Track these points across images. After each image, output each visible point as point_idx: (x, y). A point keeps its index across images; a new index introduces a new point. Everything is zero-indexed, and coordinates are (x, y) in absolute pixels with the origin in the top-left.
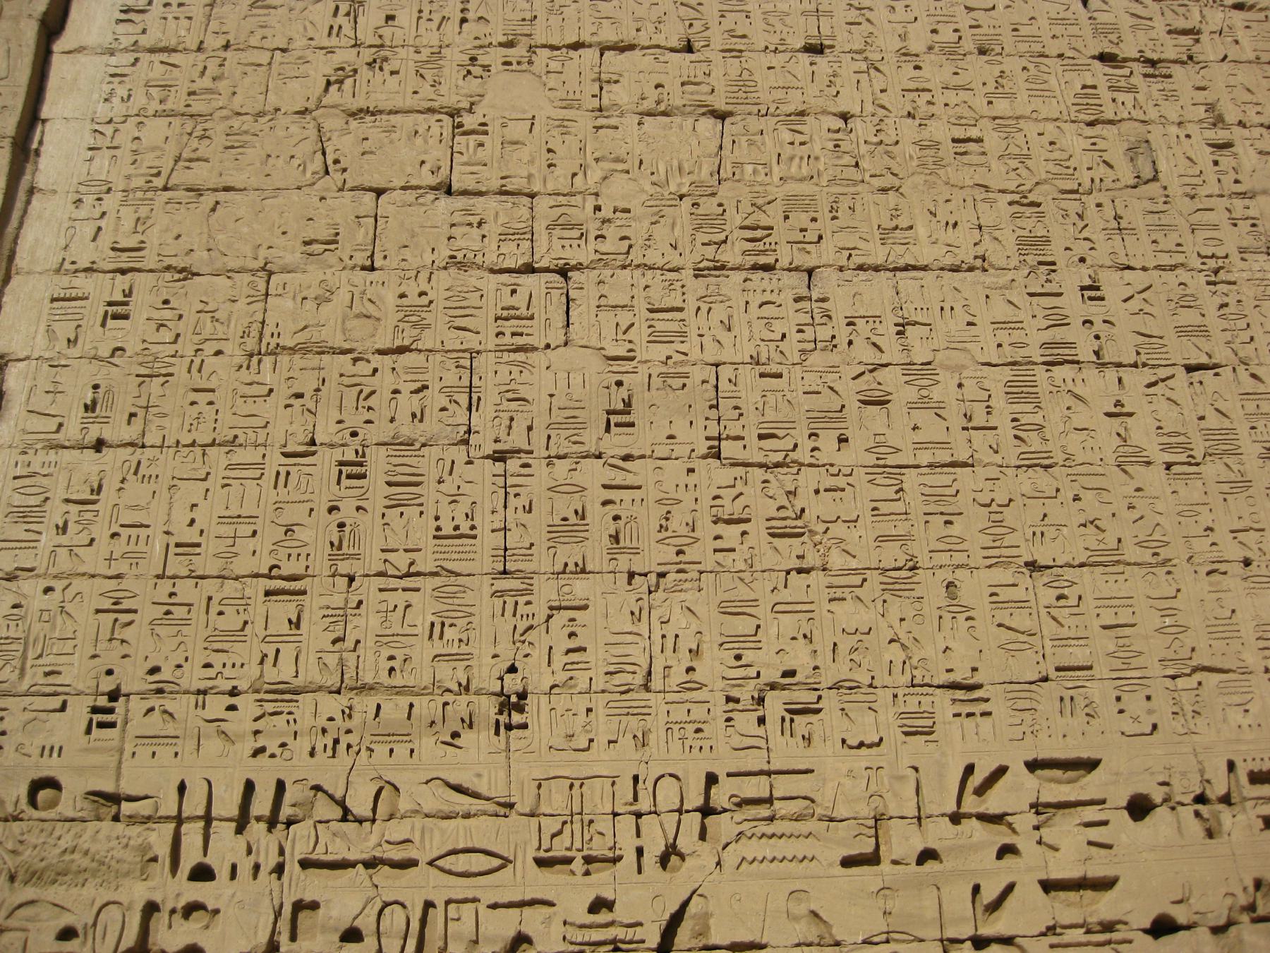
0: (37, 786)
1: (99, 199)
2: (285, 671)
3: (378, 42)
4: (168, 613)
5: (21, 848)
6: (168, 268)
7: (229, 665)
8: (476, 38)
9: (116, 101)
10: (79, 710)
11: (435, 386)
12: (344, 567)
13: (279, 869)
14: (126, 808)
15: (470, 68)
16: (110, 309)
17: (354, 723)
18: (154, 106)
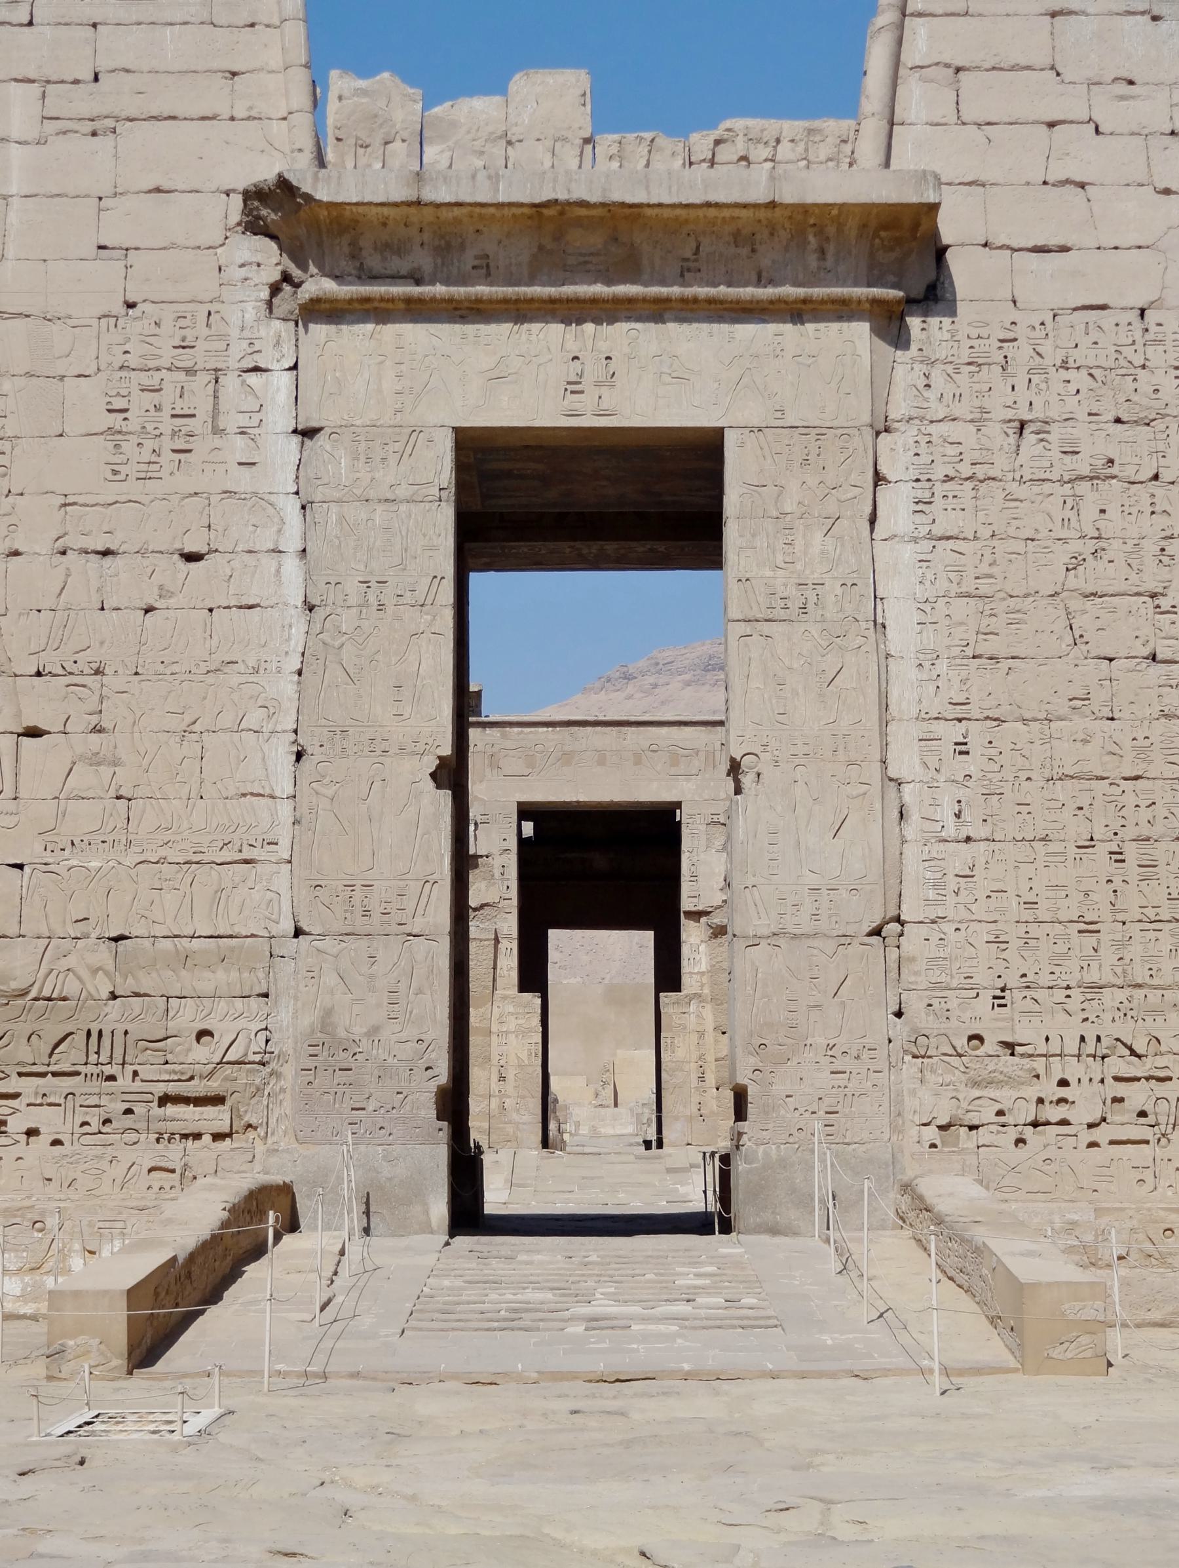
0: (971, 1038)
1: (933, 664)
2: (1093, 976)
3: (1097, 535)
4: (1026, 943)
5: (967, 1070)
6: (987, 718)
7: (1063, 973)
8: (1163, 530)
9: (928, 583)
10: (987, 997)
11: (1159, 803)
12: (1120, 917)
13: (1102, 1081)
14: (1018, 1049)
15: (1161, 557)
16: (957, 747)
17: (1134, 1005)
18: (954, 589)
